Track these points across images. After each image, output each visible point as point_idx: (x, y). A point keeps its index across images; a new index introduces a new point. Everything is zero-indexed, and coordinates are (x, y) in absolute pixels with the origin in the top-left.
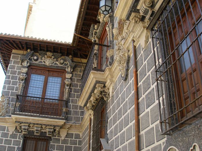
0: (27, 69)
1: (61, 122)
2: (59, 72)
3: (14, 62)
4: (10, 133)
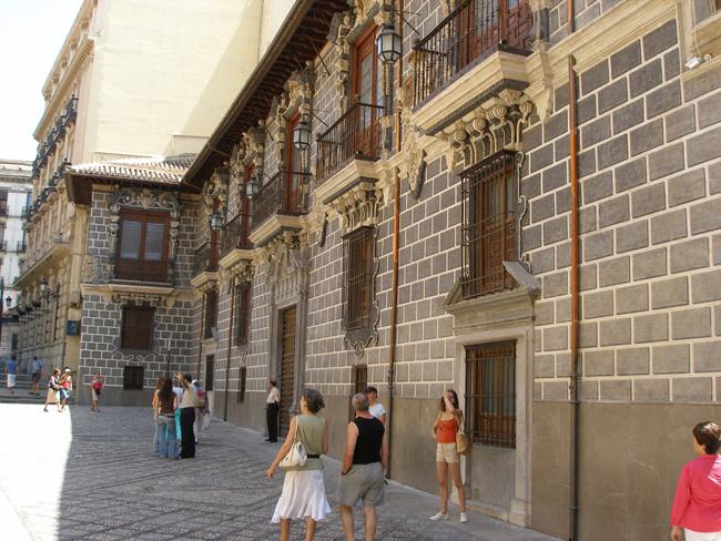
0: (118, 218)
1: (169, 290)
2: (163, 217)
3: (99, 205)
4: (106, 304)
